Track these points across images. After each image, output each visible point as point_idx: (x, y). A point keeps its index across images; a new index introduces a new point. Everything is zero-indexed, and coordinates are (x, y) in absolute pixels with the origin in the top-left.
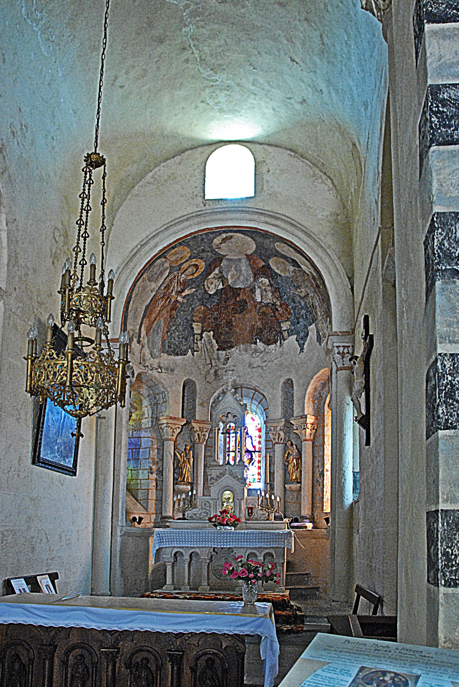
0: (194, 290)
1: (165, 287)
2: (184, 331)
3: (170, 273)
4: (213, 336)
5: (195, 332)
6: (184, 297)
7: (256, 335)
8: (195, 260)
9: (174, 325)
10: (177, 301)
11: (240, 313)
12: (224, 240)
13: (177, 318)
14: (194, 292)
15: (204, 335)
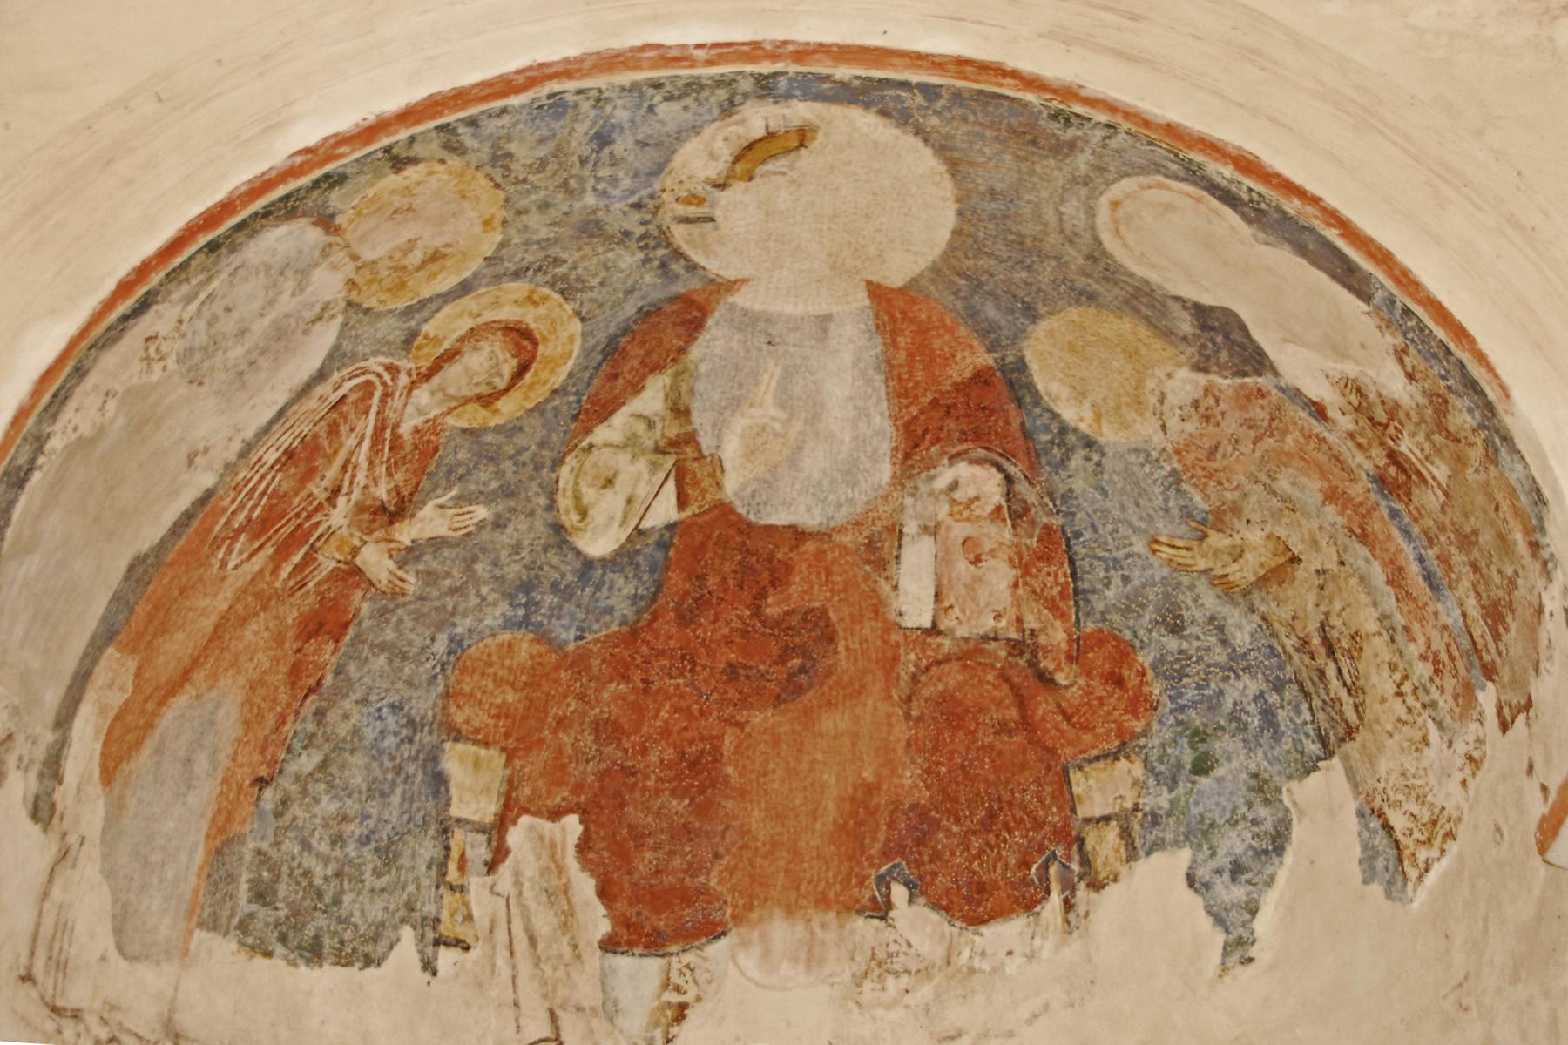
0: (482, 512)
1: (290, 454)
2: (379, 792)
3: (336, 357)
4: (584, 846)
5: (455, 811)
6: (409, 555)
7: (886, 854)
8: (519, 288)
9: (310, 742)
10: (351, 574)
11: (778, 700)
12: (752, 155)
13: (340, 693)
15: (516, 837)
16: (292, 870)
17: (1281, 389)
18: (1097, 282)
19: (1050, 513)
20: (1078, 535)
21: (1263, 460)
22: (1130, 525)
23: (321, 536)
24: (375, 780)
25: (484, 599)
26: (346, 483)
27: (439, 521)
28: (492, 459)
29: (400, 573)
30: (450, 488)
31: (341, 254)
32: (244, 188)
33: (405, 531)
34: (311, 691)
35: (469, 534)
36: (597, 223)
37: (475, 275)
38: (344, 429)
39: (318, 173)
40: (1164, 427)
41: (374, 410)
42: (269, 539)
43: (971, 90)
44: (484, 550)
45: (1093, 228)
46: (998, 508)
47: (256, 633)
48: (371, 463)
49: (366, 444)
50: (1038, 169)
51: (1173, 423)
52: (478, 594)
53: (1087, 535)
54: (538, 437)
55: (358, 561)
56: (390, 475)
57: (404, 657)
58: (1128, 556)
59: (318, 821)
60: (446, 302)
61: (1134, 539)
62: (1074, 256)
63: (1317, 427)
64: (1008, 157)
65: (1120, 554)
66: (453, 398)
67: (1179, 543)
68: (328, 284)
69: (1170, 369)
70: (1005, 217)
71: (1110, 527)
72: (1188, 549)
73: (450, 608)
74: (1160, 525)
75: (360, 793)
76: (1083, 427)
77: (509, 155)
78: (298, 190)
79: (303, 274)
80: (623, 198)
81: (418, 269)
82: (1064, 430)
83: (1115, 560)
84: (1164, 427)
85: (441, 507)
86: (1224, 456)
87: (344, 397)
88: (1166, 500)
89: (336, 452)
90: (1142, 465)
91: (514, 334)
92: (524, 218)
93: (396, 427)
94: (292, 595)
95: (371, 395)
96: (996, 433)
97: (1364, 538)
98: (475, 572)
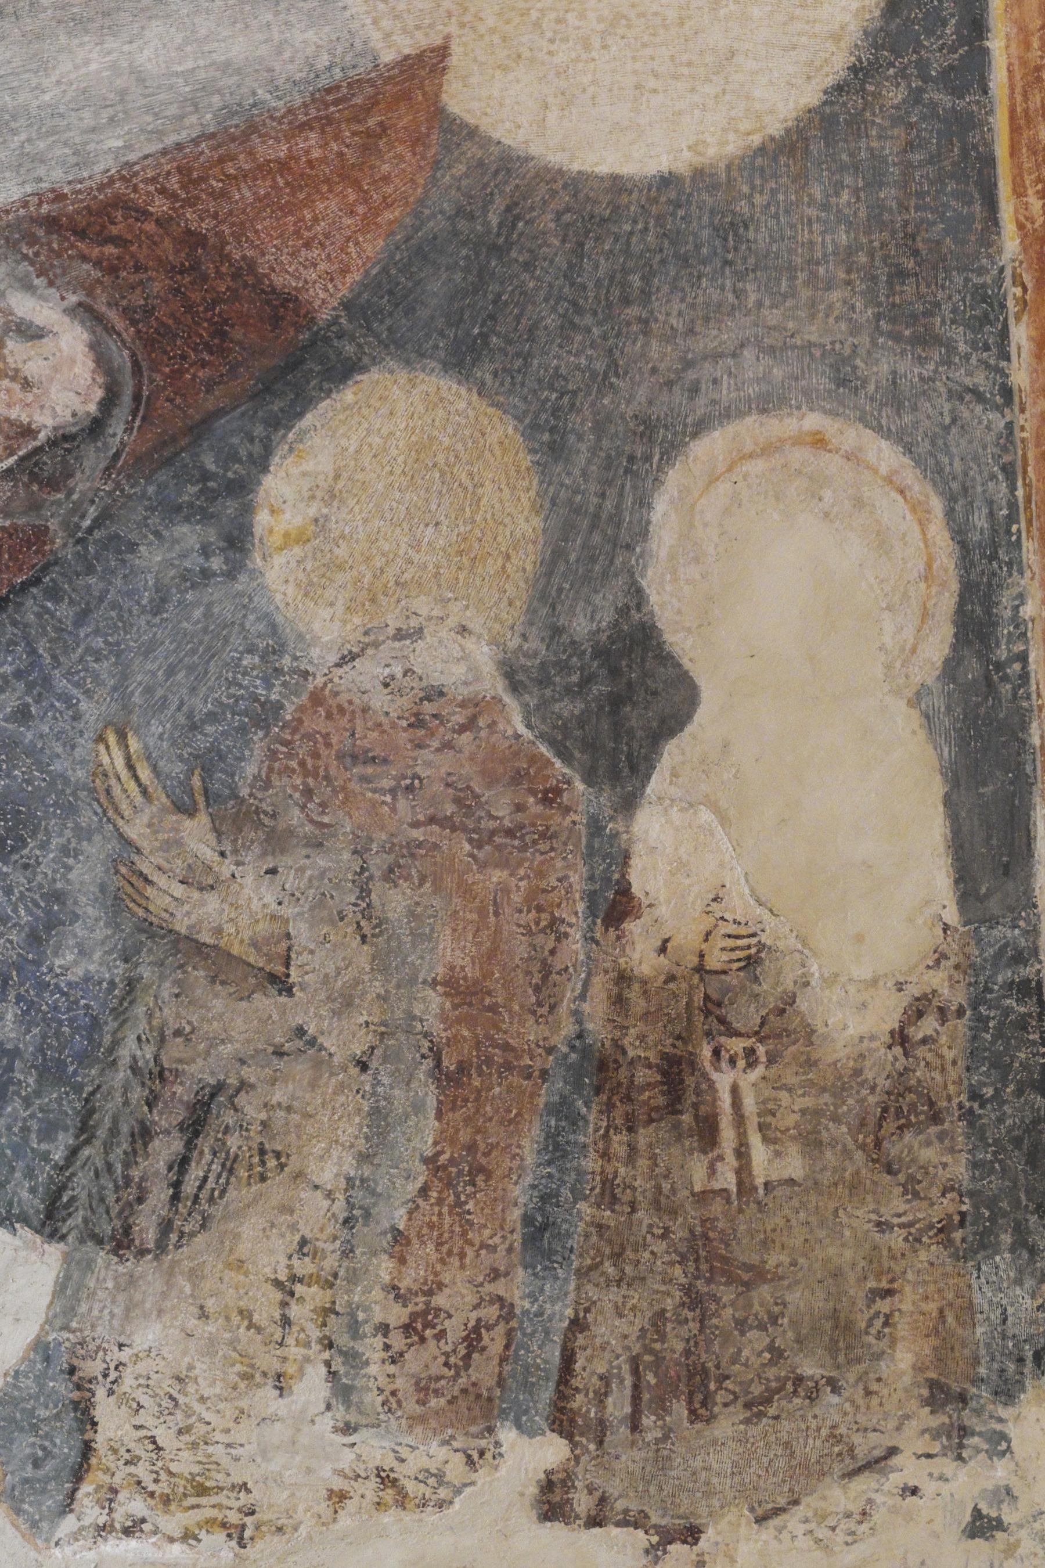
17: (596, 827)
18: (594, 451)
19: (70, 529)
20: (54, 594)
21: (412, 848)
22: (125, 676)
40: (348, 659)
43: (989, 145)
45: (727, 415)
46: (28, 432)
50: (835, 295)
51: (368, 671)
53: (65, 612)
58: (66, 699)
61: (102, 692)
62: (635, 396)
63: (575, 915)
64: (843, 238)
65: (62, 684)
67: (145, 774)
69: (476, 625)
70: (684, 261)
71: (99, 642)
72: (144, 792)
74: (156, 728)
76: (262, 519)
82: (242, 489)
83: (46, 681)
84: (348, 659)
86: (364, 779)
88: (212, 717)
90: (251, 650)
96: (176, 375)
97: (451, 1080)
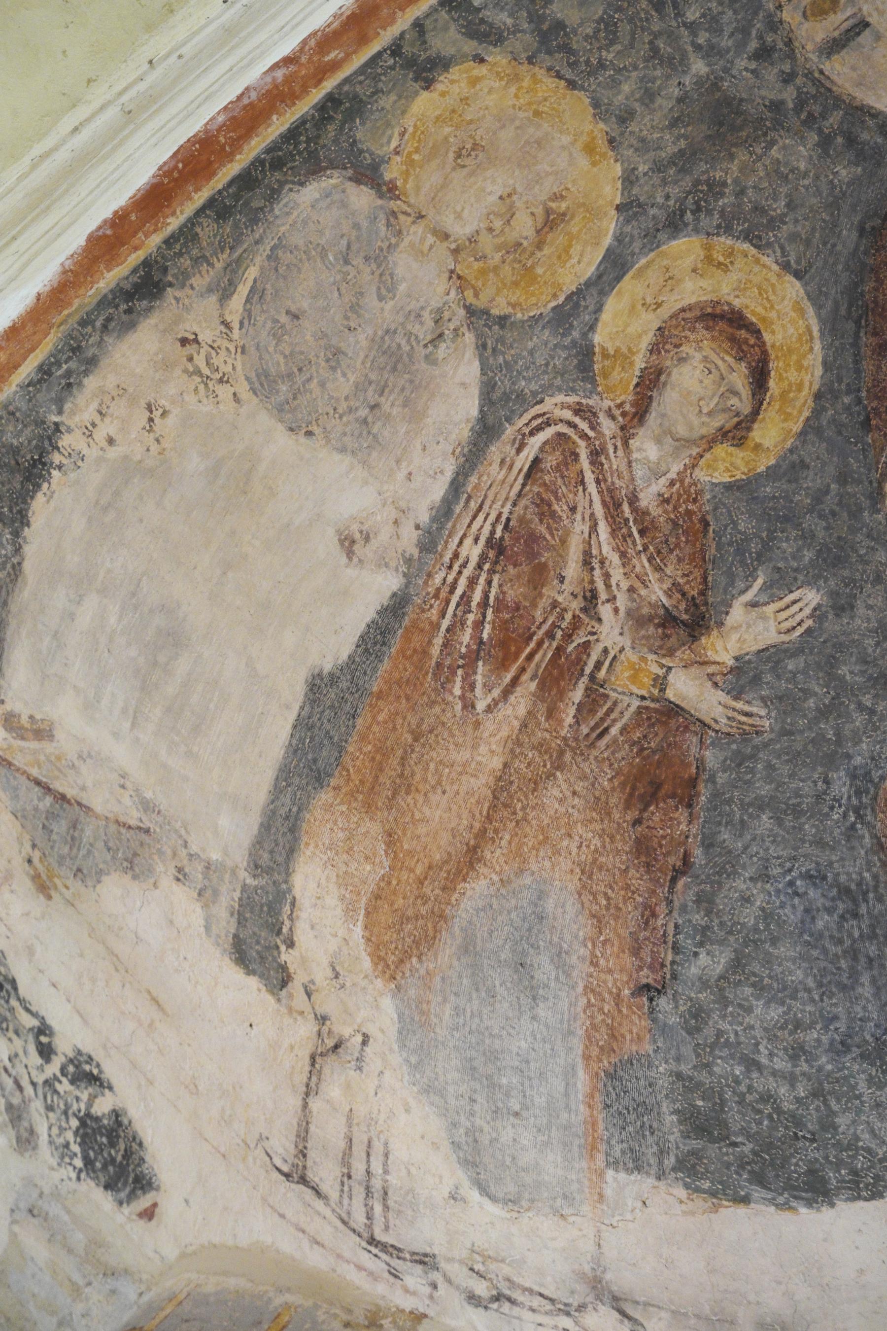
6: (742, 677)
9: (704, 936)
10: (668, 714)
14: (818, 613)
16: (742, 1096)
23: (598, 665)
24: (824, 972)
25: (872, 712)
26: (600, 585)
27: (761, 625)
28: (786, 519)
29: (739, 705)
30: (751, 576)
31: (418, 230)
32: (221, 119)
33: (719, 645)
34: (677, 874)
35: (809, 631)
36: (728, 101)
37: (619, 239)
38: (560, 508)
39: (317, 95)
41: (589, 477)
42: (523, 670)
44: (840, 647)
47: (561, 801)
48: (623, 555)
49: (603, 529)
52: (861, 707)
54: (831, 470)
55: (670, 694)
56: (658, 569)
57: (797, 812)
59: (758, 1033)
60: (604, 293)
66: (690, 442)
68: (421, 278)
73: (830, 735)
75: (808, 990)
77: (560, 25)
78: (303, 121)
79: (379, 259)
80: (741, 46)
81: (540, 245)
85: (754, 605)
87: (536, 461)
89: (563, 541)
91: (722, 325)
92: (633, 127)
93: (633, 500)
94: (592, 745)
95: (576, 456)
98: (842, 679)
